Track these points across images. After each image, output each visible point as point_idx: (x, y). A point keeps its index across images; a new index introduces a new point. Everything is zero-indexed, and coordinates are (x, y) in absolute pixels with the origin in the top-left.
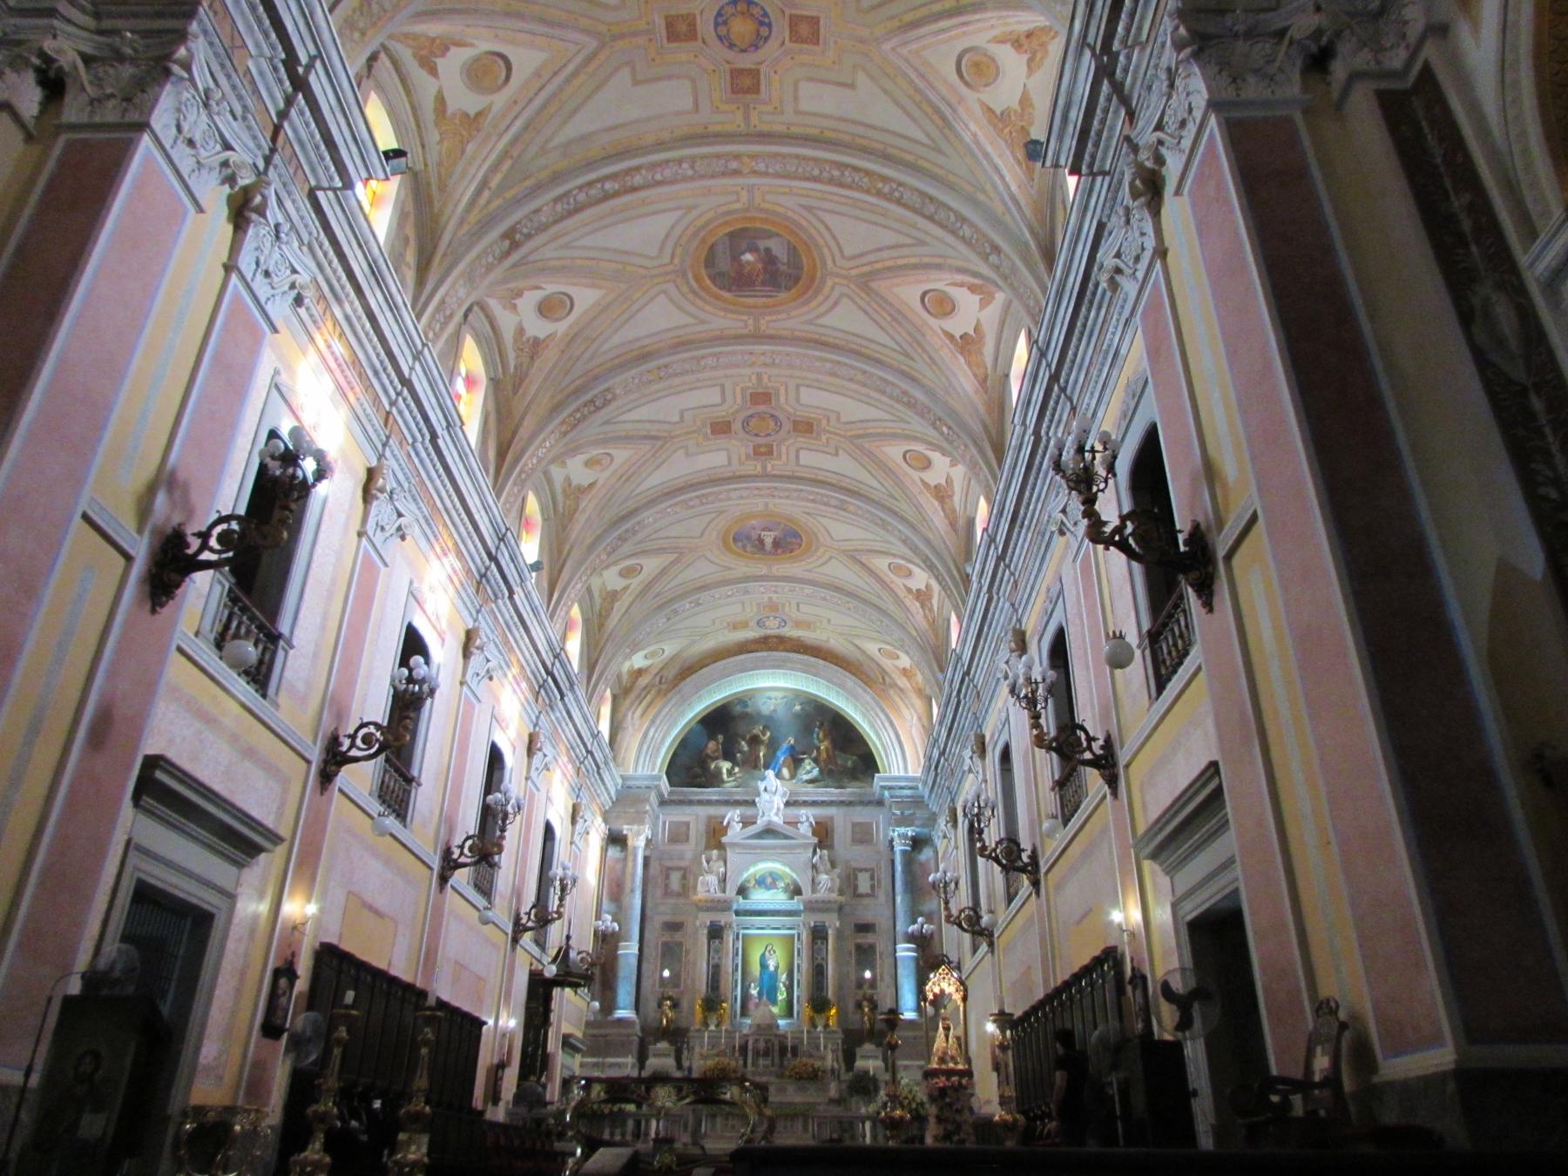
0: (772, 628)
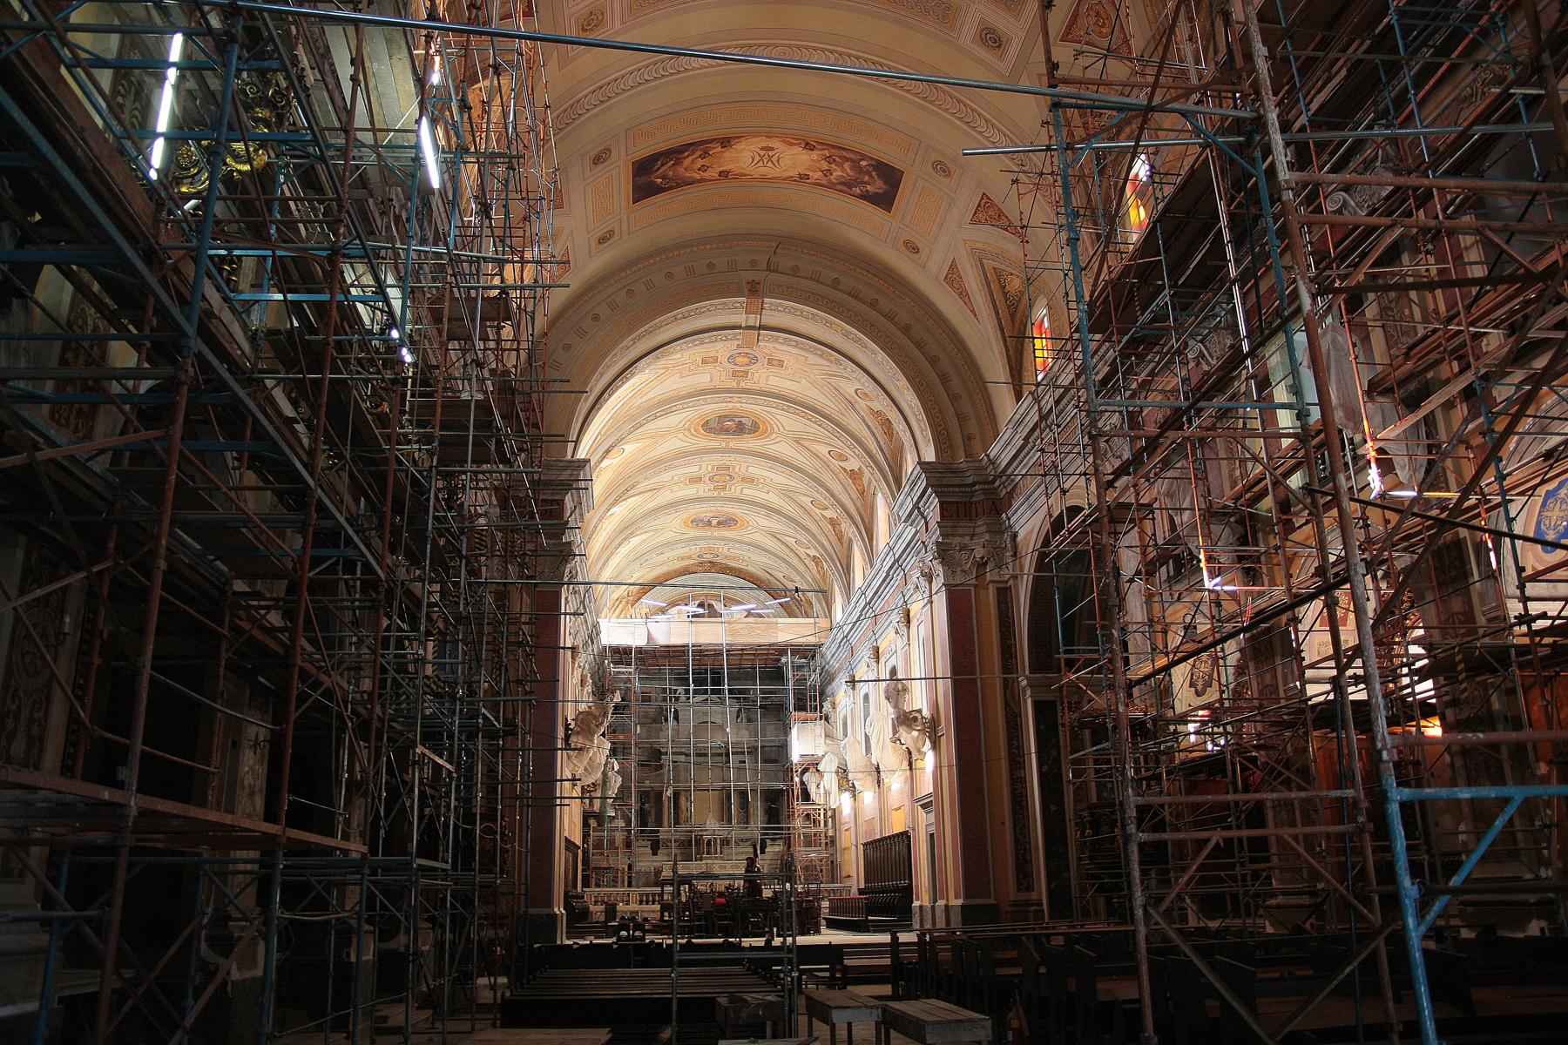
0: (708, 557)
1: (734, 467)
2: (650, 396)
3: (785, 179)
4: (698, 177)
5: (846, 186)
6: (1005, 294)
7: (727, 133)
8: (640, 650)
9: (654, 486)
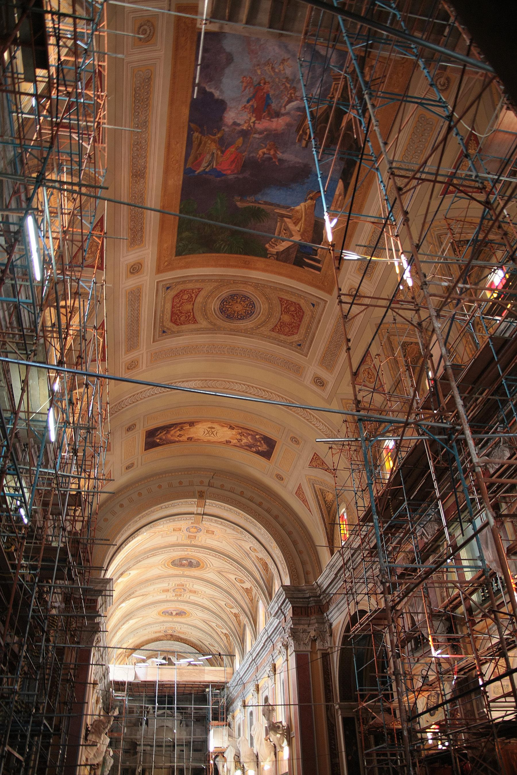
0: (170, 632)
1: (186, 585)
2: (145, 546)
3: (220, 442)
4: (177, 440)
5: (249, 447)
6: (325, 502)
7: (192, 419)
8: (130, 683)
9: (144, 593)
